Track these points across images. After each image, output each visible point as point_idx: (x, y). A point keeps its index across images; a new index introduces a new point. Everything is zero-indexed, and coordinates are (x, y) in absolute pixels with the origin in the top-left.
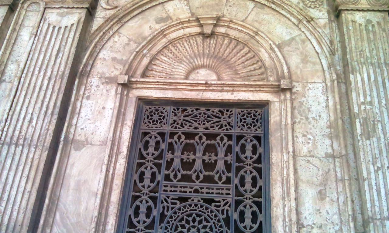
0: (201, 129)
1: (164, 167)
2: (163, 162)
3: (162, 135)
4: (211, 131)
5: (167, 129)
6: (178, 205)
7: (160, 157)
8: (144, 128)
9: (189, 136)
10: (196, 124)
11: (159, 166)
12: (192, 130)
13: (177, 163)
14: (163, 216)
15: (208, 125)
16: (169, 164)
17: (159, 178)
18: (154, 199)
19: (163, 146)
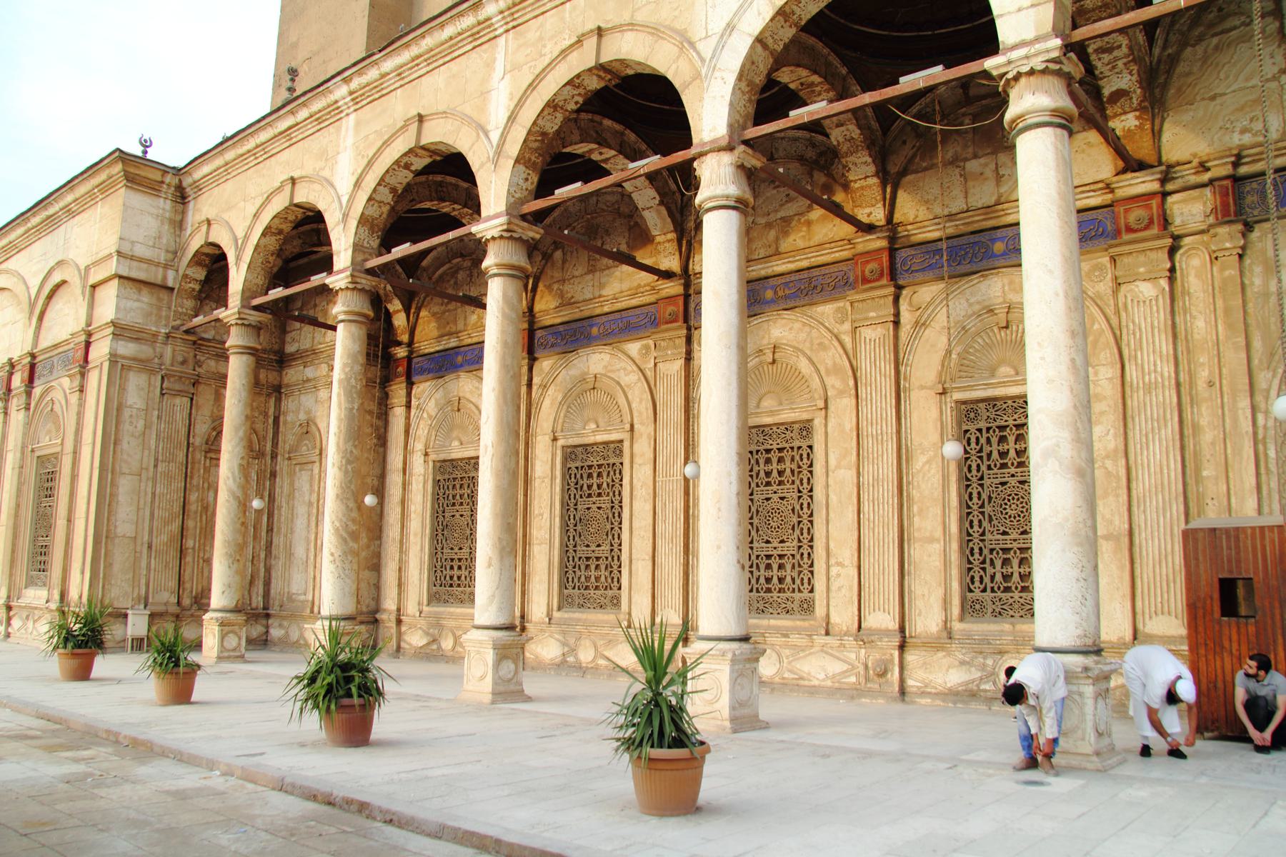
0: (1011, 422)
1: (985, 458)
2: (984, 454)
3: (980, 430)
4: (1018, 422)
5: (983, 425)
6: (1001, 488)
7: (981, 451)
8: (965, 427)
9: (1002, 428)
10: (1005, 418)
11: (981, 458)
12: (1003, 423)
13: (995, 455)
14: (990, 498)
15: (1016, 416)
16: (989, 455)
17: (983, 468)
18: (982, 485)
19: (983, 441)
